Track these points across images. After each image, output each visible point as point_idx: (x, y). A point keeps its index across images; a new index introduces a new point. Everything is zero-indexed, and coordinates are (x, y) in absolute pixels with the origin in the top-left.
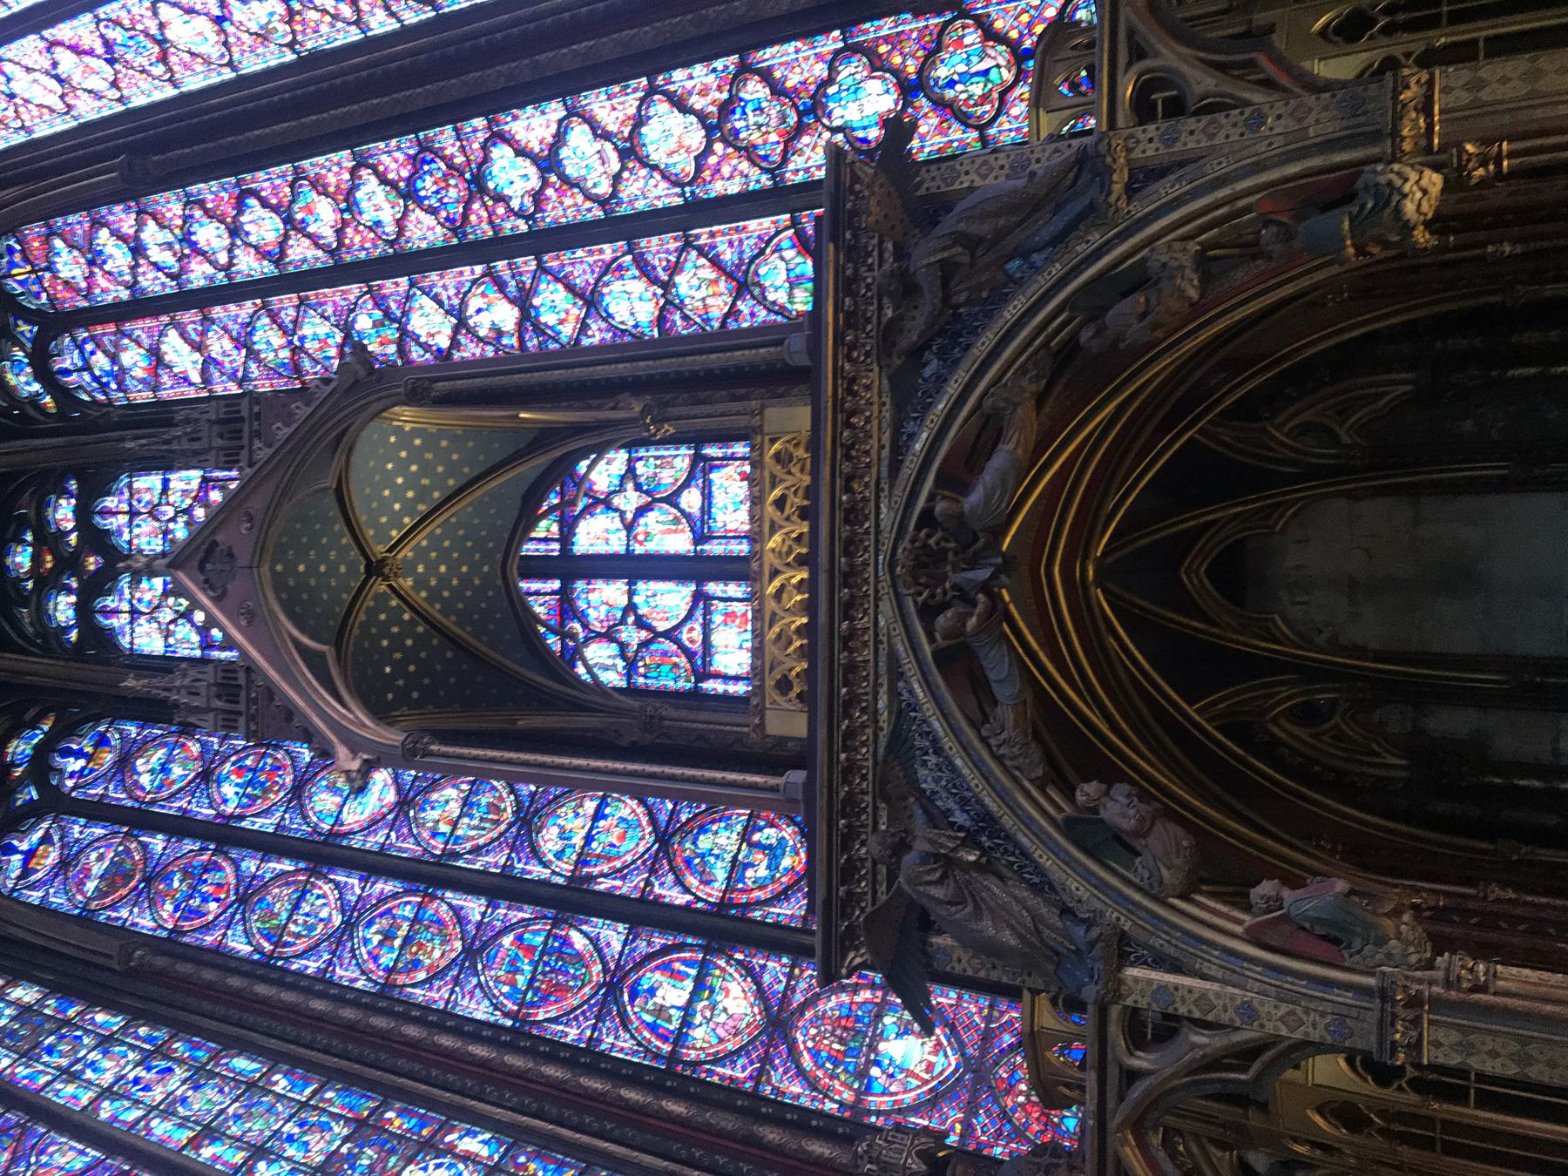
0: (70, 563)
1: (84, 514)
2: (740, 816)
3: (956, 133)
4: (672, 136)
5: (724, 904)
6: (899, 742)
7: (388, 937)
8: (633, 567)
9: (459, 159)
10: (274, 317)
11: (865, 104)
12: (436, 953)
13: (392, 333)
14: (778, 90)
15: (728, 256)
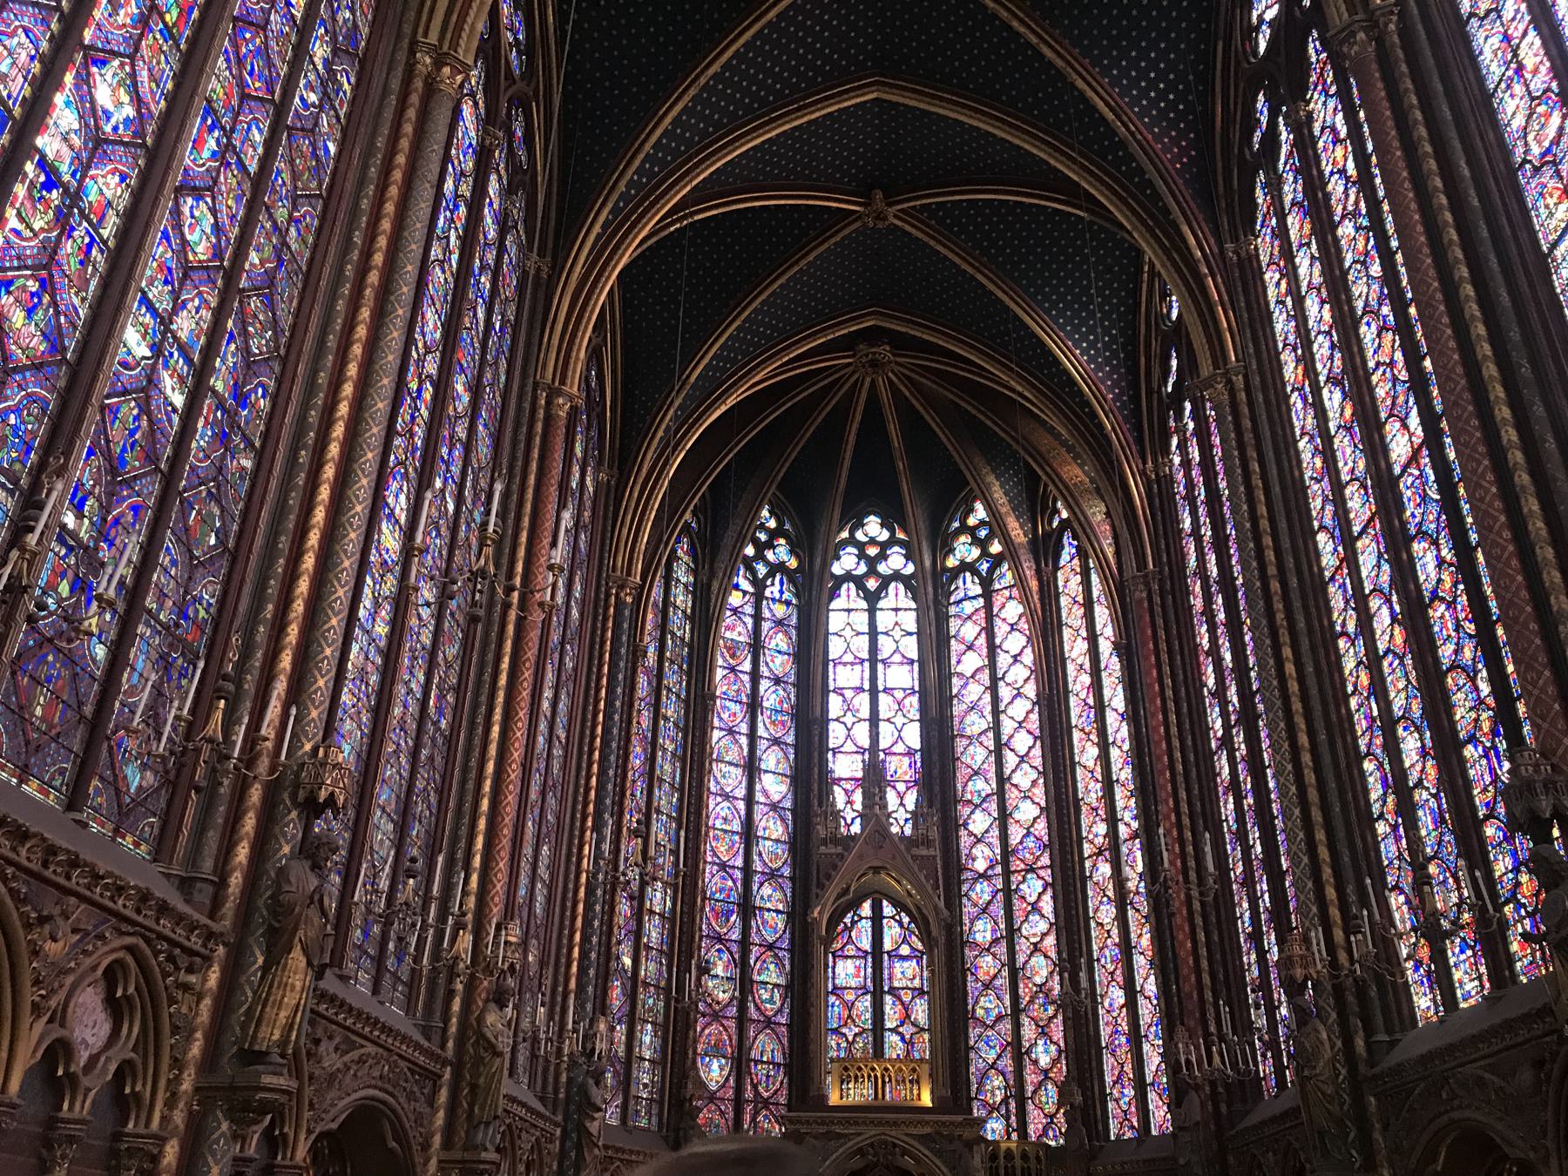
0: (872, 563)
1: (897, 576)
2: (781, 981)
3: (1030, 1089)
4: (1040, 969)
5: (752, 981)
6: (840, 1136)
7: (725, 819)
8: (877, 919)
9: (1039, 864)
10: (984, 732)
11: (1044, 1055)
12: (722, 849)
13: (976, 800)
14: (1050, 1019)
15: (998, 982)
